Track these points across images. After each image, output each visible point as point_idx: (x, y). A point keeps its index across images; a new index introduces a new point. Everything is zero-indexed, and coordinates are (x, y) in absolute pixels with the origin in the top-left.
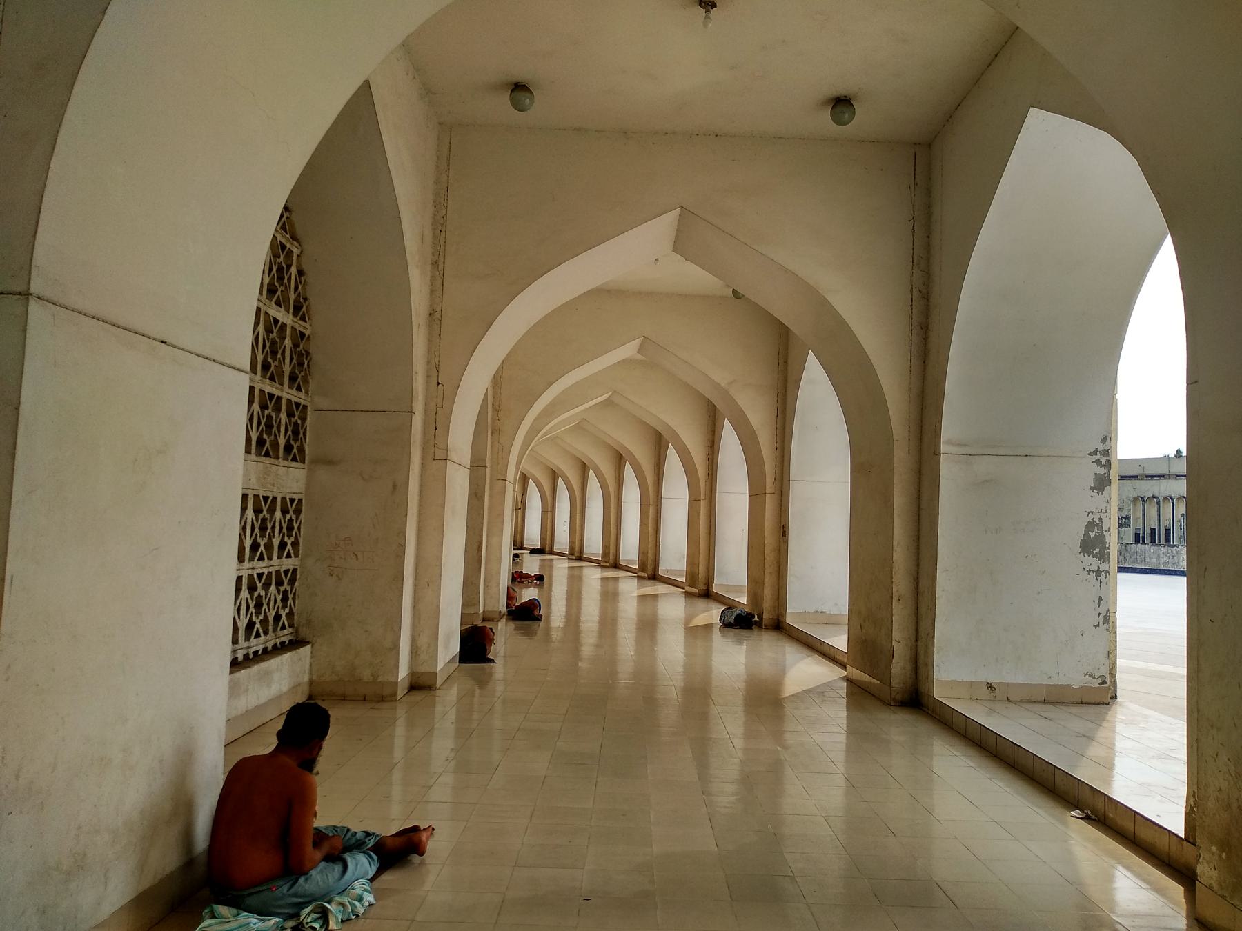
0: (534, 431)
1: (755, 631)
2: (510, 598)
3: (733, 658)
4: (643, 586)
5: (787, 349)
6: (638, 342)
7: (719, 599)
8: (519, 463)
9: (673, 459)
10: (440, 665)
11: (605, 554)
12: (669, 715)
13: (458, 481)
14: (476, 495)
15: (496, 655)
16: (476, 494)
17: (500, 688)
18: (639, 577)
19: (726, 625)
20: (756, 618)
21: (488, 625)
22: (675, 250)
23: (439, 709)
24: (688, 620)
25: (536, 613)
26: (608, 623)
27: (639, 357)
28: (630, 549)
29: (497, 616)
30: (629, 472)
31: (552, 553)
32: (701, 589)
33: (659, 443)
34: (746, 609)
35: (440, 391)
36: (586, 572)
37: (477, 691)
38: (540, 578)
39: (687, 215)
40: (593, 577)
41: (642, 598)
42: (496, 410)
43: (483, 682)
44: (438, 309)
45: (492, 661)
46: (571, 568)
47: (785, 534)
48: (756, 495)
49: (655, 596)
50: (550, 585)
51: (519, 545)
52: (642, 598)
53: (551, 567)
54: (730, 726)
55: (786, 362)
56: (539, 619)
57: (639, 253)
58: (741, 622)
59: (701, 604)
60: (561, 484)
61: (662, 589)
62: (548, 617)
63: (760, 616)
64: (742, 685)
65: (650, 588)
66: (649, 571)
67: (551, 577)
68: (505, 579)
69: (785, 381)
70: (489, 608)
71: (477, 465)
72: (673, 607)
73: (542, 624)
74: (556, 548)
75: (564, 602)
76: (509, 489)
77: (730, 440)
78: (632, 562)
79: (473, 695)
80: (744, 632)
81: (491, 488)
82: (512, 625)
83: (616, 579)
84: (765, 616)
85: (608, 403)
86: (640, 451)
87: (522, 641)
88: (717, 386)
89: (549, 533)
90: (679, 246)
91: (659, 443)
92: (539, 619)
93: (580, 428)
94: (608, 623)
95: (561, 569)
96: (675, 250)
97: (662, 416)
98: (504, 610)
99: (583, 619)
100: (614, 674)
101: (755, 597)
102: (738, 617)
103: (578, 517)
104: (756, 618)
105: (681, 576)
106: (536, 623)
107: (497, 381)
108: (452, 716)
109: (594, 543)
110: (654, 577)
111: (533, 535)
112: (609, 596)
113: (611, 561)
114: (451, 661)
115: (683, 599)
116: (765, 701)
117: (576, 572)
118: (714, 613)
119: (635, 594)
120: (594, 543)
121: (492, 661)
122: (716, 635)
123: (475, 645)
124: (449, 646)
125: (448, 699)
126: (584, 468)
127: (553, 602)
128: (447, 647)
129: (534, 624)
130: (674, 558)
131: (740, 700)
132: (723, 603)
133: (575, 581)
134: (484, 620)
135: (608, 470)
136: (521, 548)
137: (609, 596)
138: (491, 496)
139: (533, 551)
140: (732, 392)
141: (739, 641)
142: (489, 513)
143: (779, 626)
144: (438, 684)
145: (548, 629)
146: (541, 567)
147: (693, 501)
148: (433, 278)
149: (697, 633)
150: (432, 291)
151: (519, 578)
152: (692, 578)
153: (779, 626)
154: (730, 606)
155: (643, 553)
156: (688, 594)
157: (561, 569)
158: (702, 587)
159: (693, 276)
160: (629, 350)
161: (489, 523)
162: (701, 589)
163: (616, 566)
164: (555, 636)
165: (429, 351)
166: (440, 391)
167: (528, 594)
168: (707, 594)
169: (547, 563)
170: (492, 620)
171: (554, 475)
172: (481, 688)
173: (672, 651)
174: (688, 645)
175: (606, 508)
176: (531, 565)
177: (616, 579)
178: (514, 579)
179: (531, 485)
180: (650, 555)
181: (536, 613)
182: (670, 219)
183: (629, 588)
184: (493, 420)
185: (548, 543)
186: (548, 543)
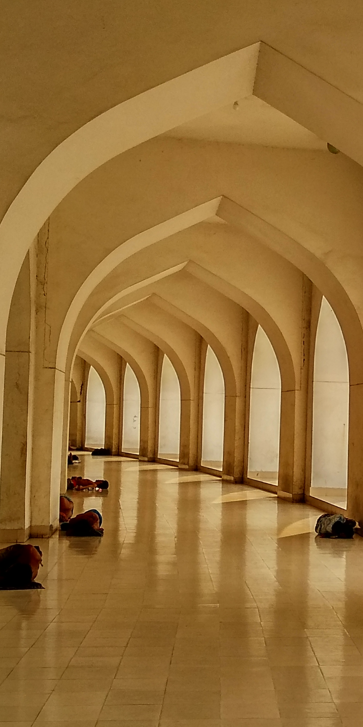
0: (91, 307)
2: (65, 509)
4: (228, 492)
6: (216, 202)
7: (316, 504)
11: (184, 455)
12: (258, 644)
16: (17, 385)
18: (224, 482)
19: (323, 535)
20: (357, 526)
21: (34, 543)
22: (256, 92)
24: (280, 529)
25: (96, 527)
26: (188, 534)
27: (223, 221)
28: (213, 450)
29: (48, 531)
30: (211, 356)
31: (119, 454)
32: (295, 493)
33: (247, 323)
34: (346, 516)
36: (161, 476)
38: (103, 485)
40: (170, 481)
41: (227, 506)
42: (41, 283)
45: (38, 586)
46: (142, 472)
49: (243, 503)
50: (118, 494)
51: (77, 443)
52: (227, 506)
53: (119, 471)
56: (100, 533)
57: (212, 95)
59: (296, 510)
61: (251, 494)
64: (341, 605)
65: (238, 494)
66: (236, 474)
67: (118, 483)
70: (37, 522)
73: (104, 539)
74: (125, 448)
75: (134, 513)
76: (60, 379)
80: (344, 542)
81: (37, 379)
82: (66, 542)
83: (197, 484)
85: (183, 275)
86: (222, 330)
88: (311, 257)
89: (115, 431)
90: (263, 85)
91: (247, 323)
92: (100, 533)
93: (151, 304)
94: (188, 534)
95: (131, 471)
96: (256, 92)
97: (249, 292)
98: (57, 524)
100: (194, 593)
102: (337, 525)
103: (150, 410)
104: (357, 526)
105: (273, 478)
106: (96, 539)
109: (170, 443)
110: (242, 481)
112: (189, 504)
113: (191, 462)
115: (275, 505)
117: (149, 477)
118: (309, 520)
120: (170, 443)
121: (38, 586)
122: (313, 546)
126: (157, 353)
129: (94, 540)
130: (265, 458)
131: (339, 618)
133: (148, 487)
134: (31, 536)
136: (82, 448)
137: (189, 504)
139: (96, 453)
140: (330, 264)
141: (337, 553)
142: (35, 408)
145: (115, 546)
146: (107, 471)
149: (291, 545)
151: (77, 485)
152: (286, 480)
154: (327, 511)
155: (228, 453)
157: (131, 471)
158: (297, 490)
160: (205, 212)
161: (34, 420)
162: (295, 493)
163: (197, 468)
164: (124, 552)
167: (92, 503)
168: (303, 499)
169: (114, 466)
171: (121, 362)
173: (263, 566)
174: (280, 561)
175: (184, 400)
176: (94, 469)
177: (197, 484)
178: (70, 487)
179: (93, 372)
180: (237, 456)
181: (96, 527)
183: (213, 495)
184: (38, 296)
185: (115, 442)
186: (115, 442)
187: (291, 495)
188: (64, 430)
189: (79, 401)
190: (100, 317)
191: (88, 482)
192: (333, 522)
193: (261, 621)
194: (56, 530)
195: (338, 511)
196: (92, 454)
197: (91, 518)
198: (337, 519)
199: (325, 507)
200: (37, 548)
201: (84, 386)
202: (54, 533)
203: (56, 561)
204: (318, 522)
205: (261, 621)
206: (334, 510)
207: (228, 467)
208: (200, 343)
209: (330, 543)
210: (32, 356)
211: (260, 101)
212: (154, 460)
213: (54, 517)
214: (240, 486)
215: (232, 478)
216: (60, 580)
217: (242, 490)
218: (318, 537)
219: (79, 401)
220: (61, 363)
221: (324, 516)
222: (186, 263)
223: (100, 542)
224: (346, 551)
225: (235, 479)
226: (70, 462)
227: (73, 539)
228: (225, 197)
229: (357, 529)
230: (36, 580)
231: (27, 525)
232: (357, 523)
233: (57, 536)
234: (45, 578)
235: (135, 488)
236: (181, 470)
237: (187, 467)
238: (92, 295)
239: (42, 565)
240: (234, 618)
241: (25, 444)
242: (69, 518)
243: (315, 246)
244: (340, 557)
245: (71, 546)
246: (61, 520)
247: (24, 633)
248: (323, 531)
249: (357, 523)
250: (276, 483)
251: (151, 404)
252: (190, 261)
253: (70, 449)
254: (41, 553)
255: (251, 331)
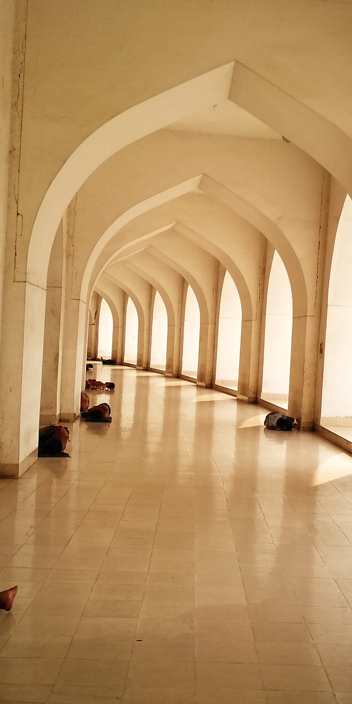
0: (105, 256)
1: (294, 433)
2: (84, 400)
3: (276, 454)
4: (201, 394)
5: (329, 189)
6: (197, 179)
7: (265, 405)
8: (91, 284)
9: (229, 284)
10: (22, 458)
11: (169, 366)
12: (221, 502)
13: (36, 302)
14: (52, 313)
15: (70, 451)
16: (52, 311)
17: (74, 477)
18: (198, 386)
21: (64, 425)
22: (231, 97)
23: (21, 494)
24: (239, 423)
26: (171, 424)
29: (72, 417)
34: (287, 414)
35: (20, 223)
37: (55, 480)
38: (111, 386)
39: (240, 67)
40: (159, 385)
41: (200, 404)
42: (71, 237)
43: (59, 473)
44: (18, 147)
45: (67, 455)
46: (138, 377)
47: (322, 351)
48: (299, 317)
49: (212, 403)
51: (92, 356)
52: (200, 404)
53: (121, 376)
54: (271, 514)
55: (328, 201)
56: (109, 420)
57: (199, 99)
58: (282, 425)
59: (250, 409)
60: (130, 303)
61: (218, 396)
62: (119, 417)
63: (299, 420)
67: (121, 385)
68: (79, 387)
69: (327, 216)
70: (65, 411)
71: (53, 286)
72: (227, 411)
74: (126, 360)
75: (132, 407)
77: (278, 269)
78: (192, 373)
79: (51, 483)
80: (285, 434)
81: (66, 307)
82: (85, 426)
84: (303, 420)
85: (172, 232)
86: (200, 275)
87: (94, 439)
89: (119, 346)
91: (217, 270)
92: (109, 420)
93: (147, 253)
94: (171, 424)
95: (130, 376)
98: (78, 412)
99: (149, 421)
101: (295, 403)
103: (146, 333)
104: (295, 422)
105: (234, 385)
107: (71, 211)
108: (32, 500)
110: (211, 386)
111: (105, 350)
112: (172, 402)
114: (31, 455)
115: (235, 405)
116: (301, 490)
117: (144, 381)
118: (260, 417)
119: (195, 400)
121: (67, 455)
123: (52, 442)
124: (30, 442)
125: (29, 487)
126: (151, 290)
127: (123, 407)
128: (27, 442)
130: (228, 372)
132: (270, 410)
133: (143, 388)
134: (60, 421)
135: (173, 293)
136: (95, 359)
137: (172, 402)
138: (66, 314)
139: (105, 362)
141: (280, 441)
143: (315, 429)
144: (20, 474)
145: (118, 429)
146: (113, 376)
147: (246, 321)
148: (13, 119)
149: (245, 434)
150: (12, 131)
151: (92, 385)
152: (243, 387)
153: (315, 429)
155: (201, 366)
156: (240, 401)
157: (130, 376)
158: (251, 395)
159: (244, 121)
160: (190, 185)
161: (64, 338)
163: (179, 376)
164: (125, 435)
165: (9, 185)
166: (20, 223)
167: (102, 399)
168: (256, 401)
169: (118, 373)
170: (67, 421)
171: (124, 296)
172: (57, 477)
173: (225, 450)
175: (171, 325)
176: (104, 375)
177: (179, 387)
178: (87, 387)
179: (104, 304)
181: (106, 415)
182: (226, 70)
183: (190, 395)
184: (68, 246)
187: (245, 398)
188: (85, 345)
189: (94, 324)
190: (111, 262)
191: (100, 384)
192: (278, 418)
193: (223, 484)
194: (78, 417)
195: (281, 410)
196: (103, 364)
197: (104, 408)
198: (280, 416)
199: (273, 407)
200: (66, 428)
201: (97, 313)
202: (76, 419)
203: (78, 439)
204: (266, 418)
205: (223, 484)
206: (278, 410)
207: (201, 377)
208: (183, 284)
209: (274, 434)
210: (63, 290)
211: (233, 104)
212: (148, 369)
213: (76, 409)
214: (208, 391)
215: (204, 384)
216: (80, 452)
217: (212, 393)
218: (266, 430)
219: (94, 324)
220: (84, 296)
221: (271, 414)
222: (175, 223)
223: (109, 426)
224: (286, 440)
225: (206, 385)
226: (87, 369)
227: (90, 423)
228: (205, 175)
229: (295, 424)
230: (65, 451)
231: (58, 413)
232: (295, 420)
233: (78, 421)
234: (71, 449)
235: (134, 389)
236: (167, 377)
237: (171, 375)
238: (106, 246)
239: (69, 441)
240: (204, 484)
241: (57, 354)
242: (87, 409)
243: (271, 212)
244: (283, 444)
245: (88, 429)
246: (81, 410)
247: (54, 487)
248: (270, 425)
249: (295, 420)
250: (235, 388)
251: (146, 328)
252: (178, 222)
253: (88, 360)
254: (68, 432)
255: (220, 277)
